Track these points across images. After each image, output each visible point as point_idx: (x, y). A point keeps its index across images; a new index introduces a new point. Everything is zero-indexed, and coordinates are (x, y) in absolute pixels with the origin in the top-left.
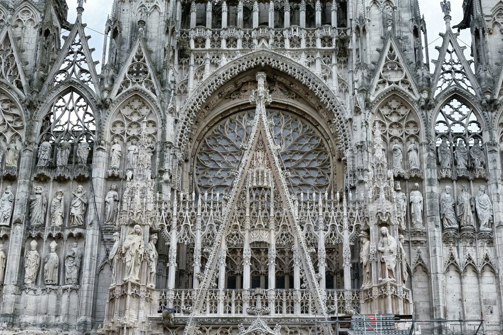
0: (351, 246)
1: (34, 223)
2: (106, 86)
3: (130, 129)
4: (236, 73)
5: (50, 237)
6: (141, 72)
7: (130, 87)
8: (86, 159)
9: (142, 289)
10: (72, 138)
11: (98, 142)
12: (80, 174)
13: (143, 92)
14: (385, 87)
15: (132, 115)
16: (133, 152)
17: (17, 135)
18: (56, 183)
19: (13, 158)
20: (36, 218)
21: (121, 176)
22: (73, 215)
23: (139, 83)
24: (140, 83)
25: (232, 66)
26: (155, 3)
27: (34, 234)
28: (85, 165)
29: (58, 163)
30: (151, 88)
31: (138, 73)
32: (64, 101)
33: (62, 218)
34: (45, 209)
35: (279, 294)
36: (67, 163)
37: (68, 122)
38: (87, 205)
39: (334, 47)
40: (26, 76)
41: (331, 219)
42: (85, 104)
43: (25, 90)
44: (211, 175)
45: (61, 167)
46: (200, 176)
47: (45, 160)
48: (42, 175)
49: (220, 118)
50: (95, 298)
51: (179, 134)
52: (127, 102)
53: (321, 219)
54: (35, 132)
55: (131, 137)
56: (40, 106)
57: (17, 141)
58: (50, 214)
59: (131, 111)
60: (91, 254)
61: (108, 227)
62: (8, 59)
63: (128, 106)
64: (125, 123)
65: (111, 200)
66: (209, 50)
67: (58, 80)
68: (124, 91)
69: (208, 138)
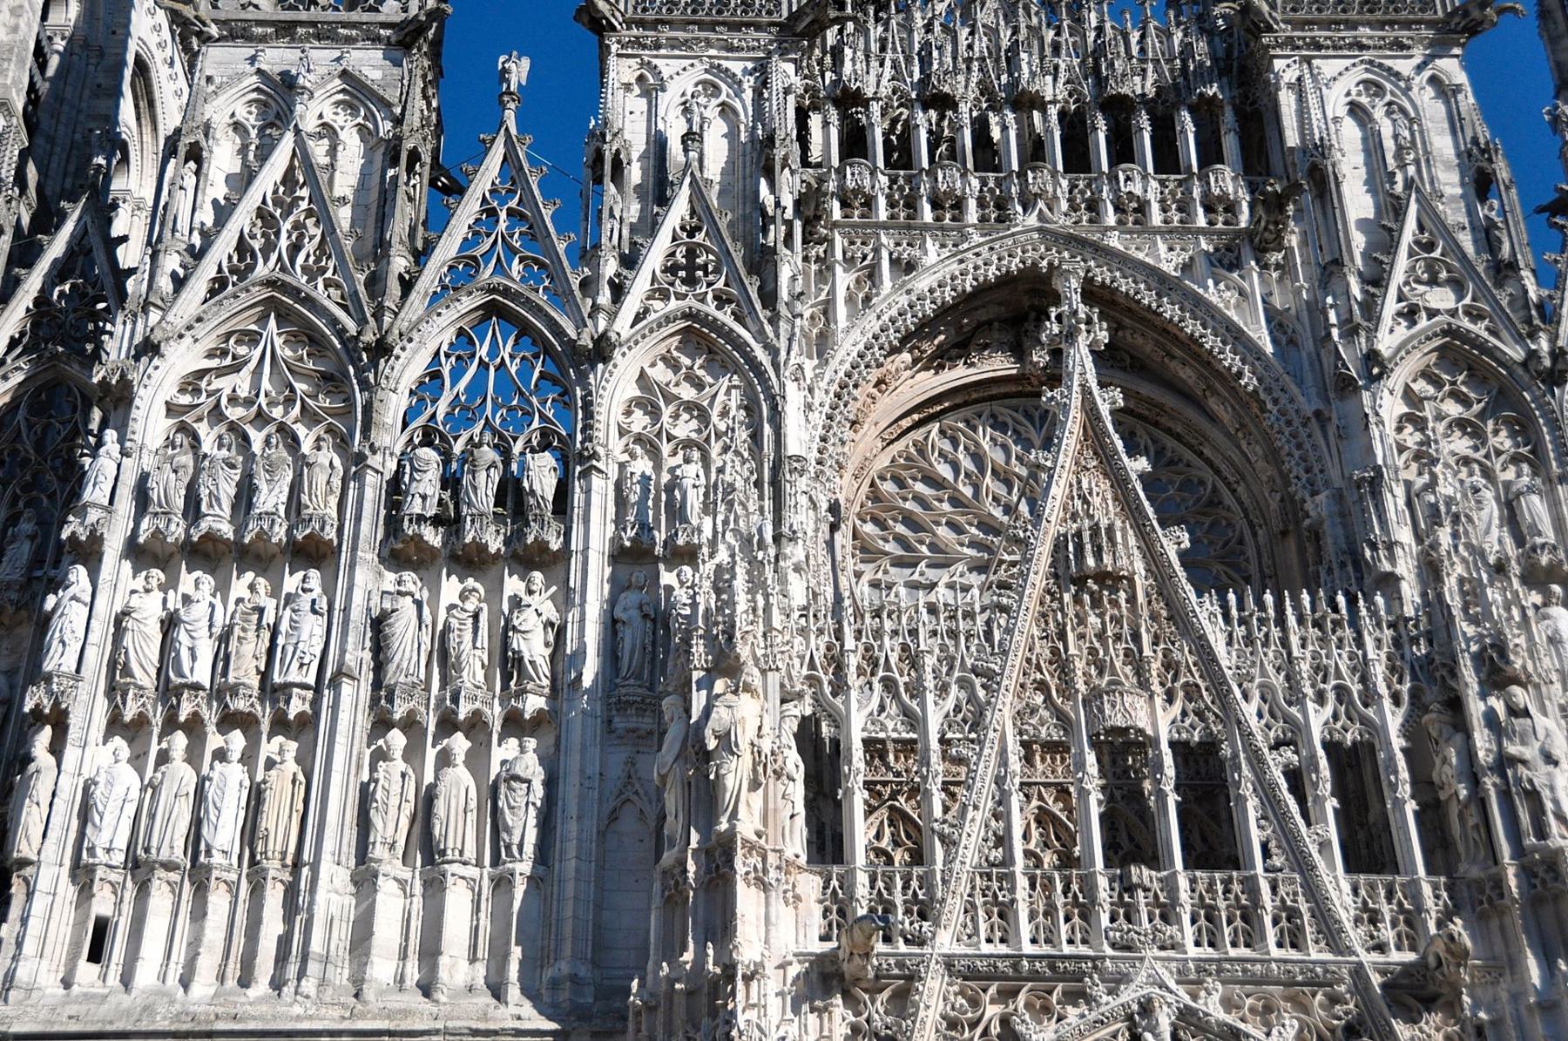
0: (1402, 750)
4: (969, 289)
5: (448, 724)
9: (772, 859)
13: (715, 326)
14: (1413, 323)
24: (703, 301)
25: (955, 268)
26: (723, 97)
27: (399, 711)
30: (733, 313)
35: (1201, 887)
39: (1243, 225)
41: (1332, 670)
44: (898, 575)
46: (865, 579)
49: (916, 417)
50: (599, 907)
51: (815, 447)
53: (1305, 667)
56: (403, 349)
60: (582, 771)
65: (635, 613)
66: (884, 226)
69: (882, 478)
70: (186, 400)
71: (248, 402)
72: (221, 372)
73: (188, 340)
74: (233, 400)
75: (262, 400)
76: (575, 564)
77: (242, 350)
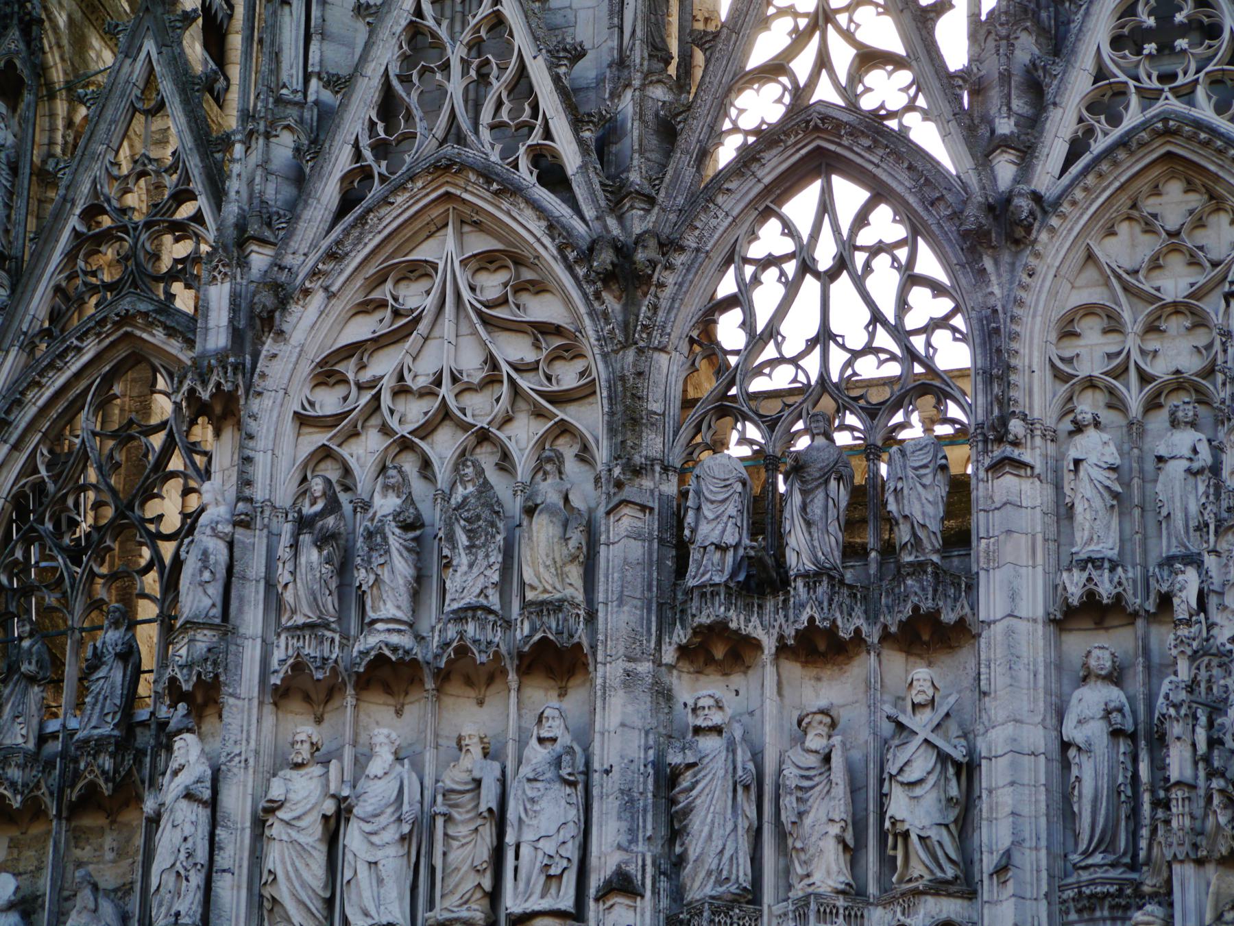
1: (699, 888)
2: (1005, 126)
3: (1152, 344)
6: (1184, 30)
7: (1133, 116)
8: (934, 526)
10: (851, 419)
11: (993, 428)
12: (916, 608)
15: (1155, 264)
16: (1185, 464)
17: (564, 429)
18: (792, 669)
19: (561, 552)
20: (711, 862)
21: (1134, 601)
22: (900, 828)
23: (1178, 93)
24: (1186, 95)
28: (935, 558)
29: (791, 559)
31: (1165, 35)
32: (789, 229)
33: (846, 847)
34: (752, 812)
36: (837, 554)
37: (824, 337)
38: (967, 770)
40: (577, 122)
42: (900, 232)
43: (580, 192)
45: (811, 579)
47: (721, 548)
48: (719, 629)
52: (1124, 200)
54: (656, 407)
55: (1166, 383)
56: (669, 267)
57: (571, 466)
58: (782, 835)
59: (1148, 246)
61: (1092, 882)
62: (476, 45)
63: (1129, 218)
64: (1127, 315)
65: (1093, 732)
67: (748, 122)
68: (1098, 145)
70: (329, 401)
71: (424, 393)
72: (379, 343)
73: (318, 298)
74: (401, 390)
75: (446, 390)
76: (992, 643)
77: (414, 296)
